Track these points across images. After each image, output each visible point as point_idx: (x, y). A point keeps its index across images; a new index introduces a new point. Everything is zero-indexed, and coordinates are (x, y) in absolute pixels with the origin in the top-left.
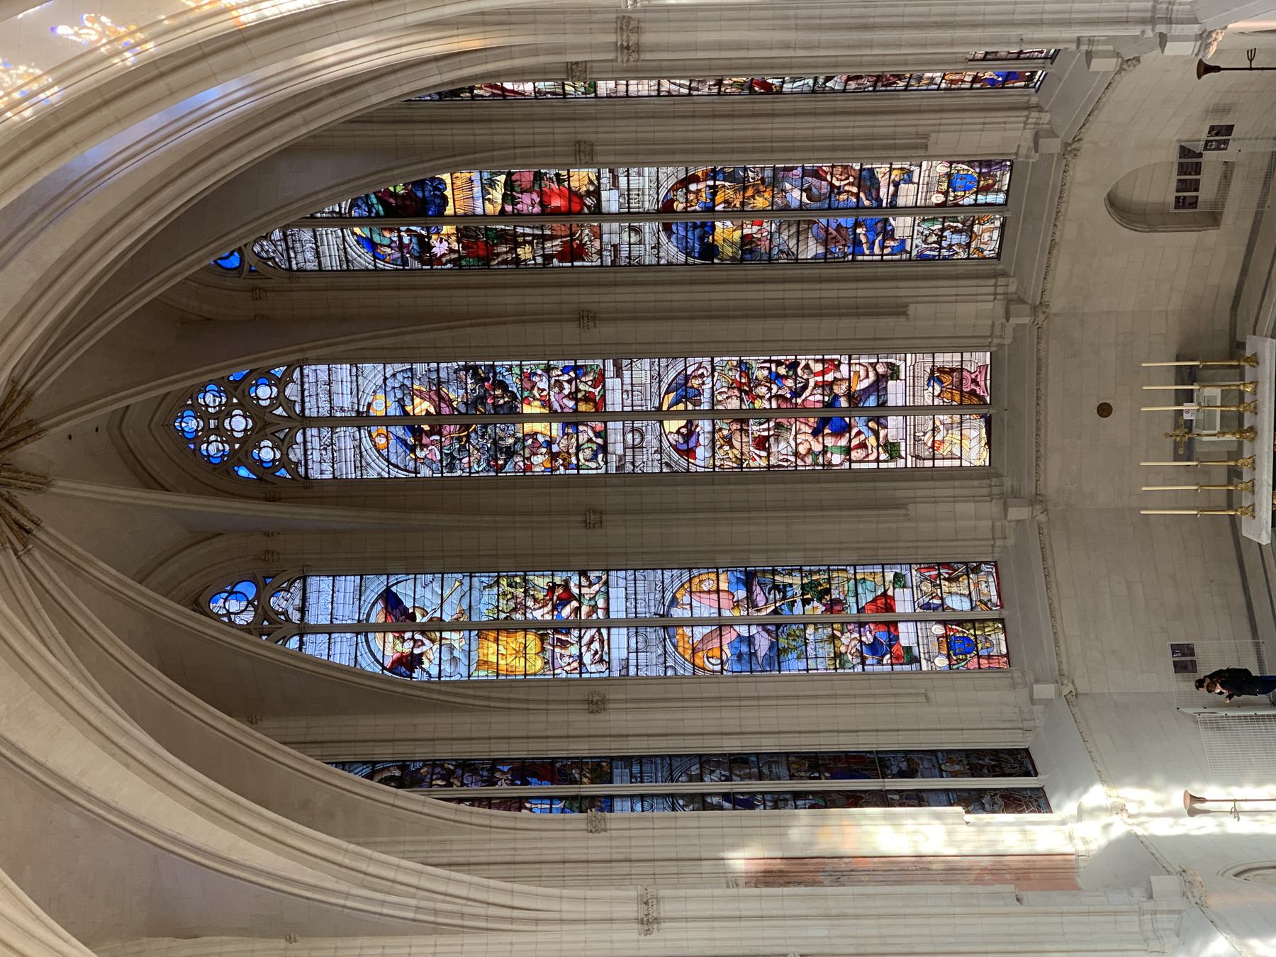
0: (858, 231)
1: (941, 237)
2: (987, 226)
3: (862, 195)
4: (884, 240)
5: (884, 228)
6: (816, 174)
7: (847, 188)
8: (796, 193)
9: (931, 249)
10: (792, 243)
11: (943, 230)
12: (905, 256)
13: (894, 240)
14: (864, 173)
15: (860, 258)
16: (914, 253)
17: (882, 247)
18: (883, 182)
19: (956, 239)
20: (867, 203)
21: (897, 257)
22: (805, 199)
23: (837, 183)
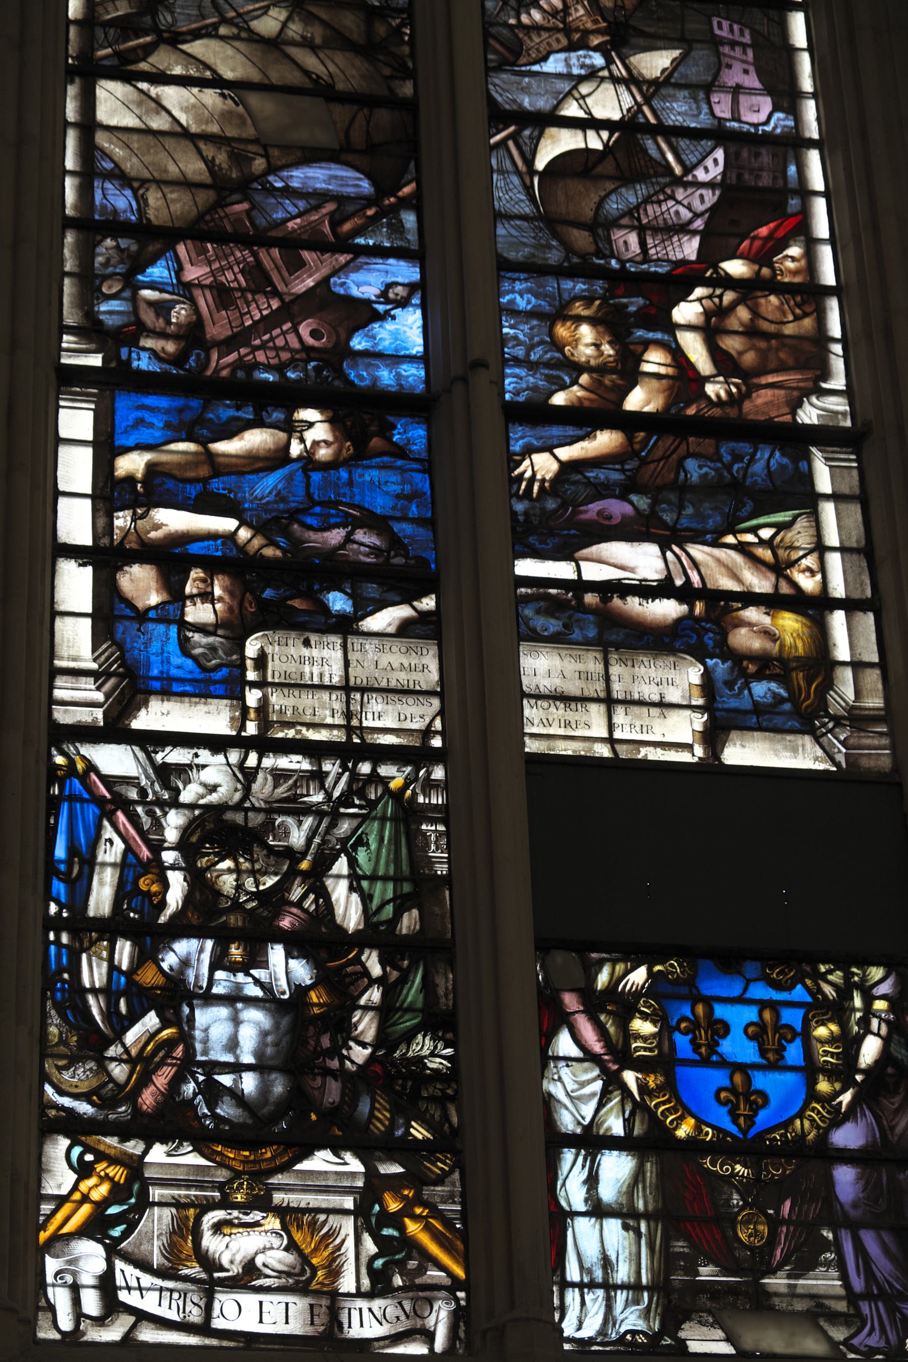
0: (317, 430)
1: (243, 932)
2: (353, 1252)
3: (605, 441)
4: (224, 559)
5: (336, 570)
6: (756, 204)
7: (655, 361)
8: (609, 103)
9: (140, 869)
10: (229, 62)
11: (318, 939)
12: (79, 700)
13: (235, 629)
14: (766, 460)
15: (76, 421)
16: (115, 760)
17: (172, 558)
18: (718, 565)
19: (232, 1033)
20: (544, 465)
21: (75, 640)
22: (556, 144)
23: (687, 312)
